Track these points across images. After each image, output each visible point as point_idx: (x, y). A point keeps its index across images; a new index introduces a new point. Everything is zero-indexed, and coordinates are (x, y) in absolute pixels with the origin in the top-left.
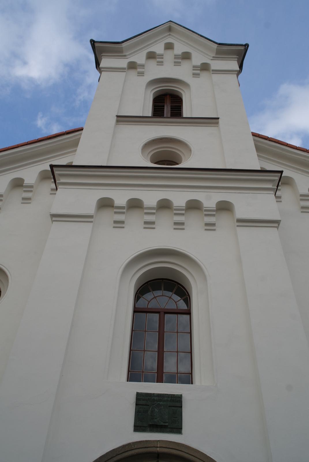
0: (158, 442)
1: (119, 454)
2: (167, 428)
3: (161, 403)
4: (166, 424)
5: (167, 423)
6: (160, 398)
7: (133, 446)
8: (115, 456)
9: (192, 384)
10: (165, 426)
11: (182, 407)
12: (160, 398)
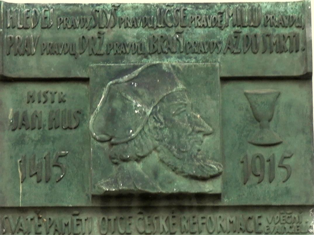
4: (208, 187)
5: (213, 177)
10: (201, 196)
12: (160, 32)
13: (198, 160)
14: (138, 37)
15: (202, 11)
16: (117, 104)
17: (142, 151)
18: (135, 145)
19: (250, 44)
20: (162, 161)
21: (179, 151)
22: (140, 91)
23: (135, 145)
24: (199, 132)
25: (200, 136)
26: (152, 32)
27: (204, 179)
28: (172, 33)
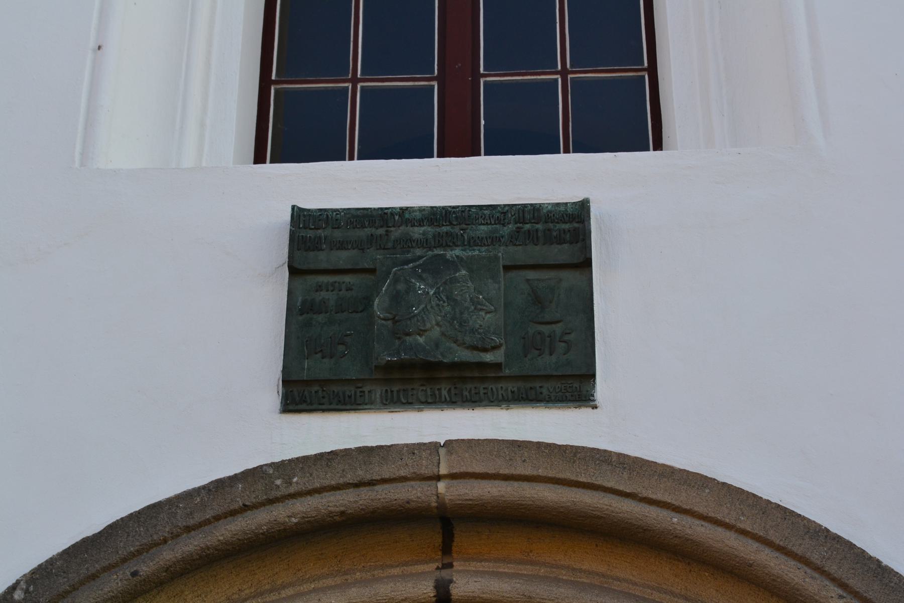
0: (442, 451)
1: (188, 529)
2: (498, 379)
3: (457, 252)
4: (488, 357)
5: (495, 348)
6: (444, 229)
7: (278, 482)
8: (165, 541)
9: (658, 146)
10: (482, 365)
11: (587, 264)
12: (444, 229)
13: (479, 334)
14: (424, 234)
15: (486, 212)
16: (401, 287)
17: (425, 325)
18: (418, 321)
19: (532, 237)
20: (443, 334)
21: (460, 325)
22: (424, 275)
23: (418, 321)
24: (481, 310)
25: (483, 313)
26: (438, 230)
27: (485, 350)
28: (457, 230)
